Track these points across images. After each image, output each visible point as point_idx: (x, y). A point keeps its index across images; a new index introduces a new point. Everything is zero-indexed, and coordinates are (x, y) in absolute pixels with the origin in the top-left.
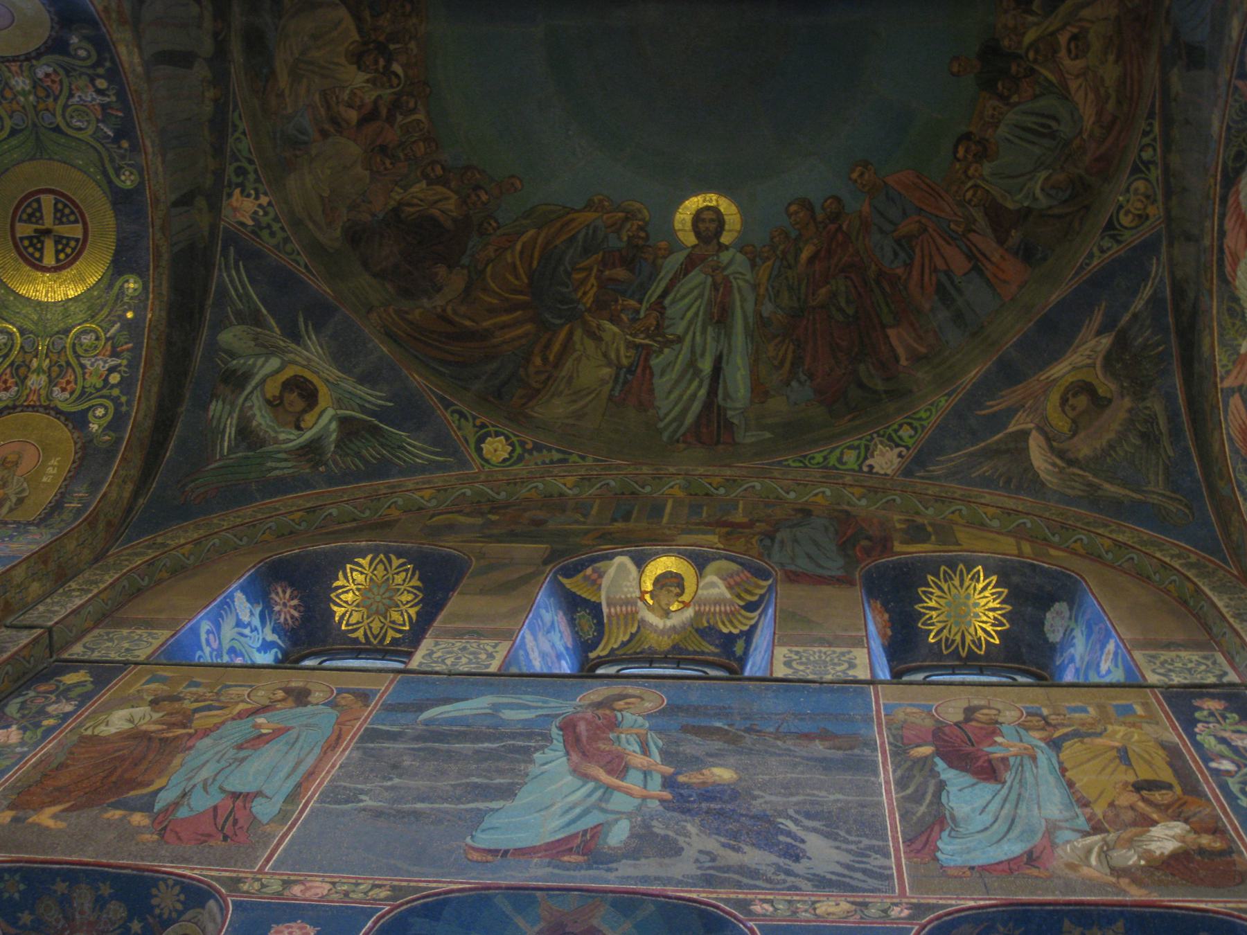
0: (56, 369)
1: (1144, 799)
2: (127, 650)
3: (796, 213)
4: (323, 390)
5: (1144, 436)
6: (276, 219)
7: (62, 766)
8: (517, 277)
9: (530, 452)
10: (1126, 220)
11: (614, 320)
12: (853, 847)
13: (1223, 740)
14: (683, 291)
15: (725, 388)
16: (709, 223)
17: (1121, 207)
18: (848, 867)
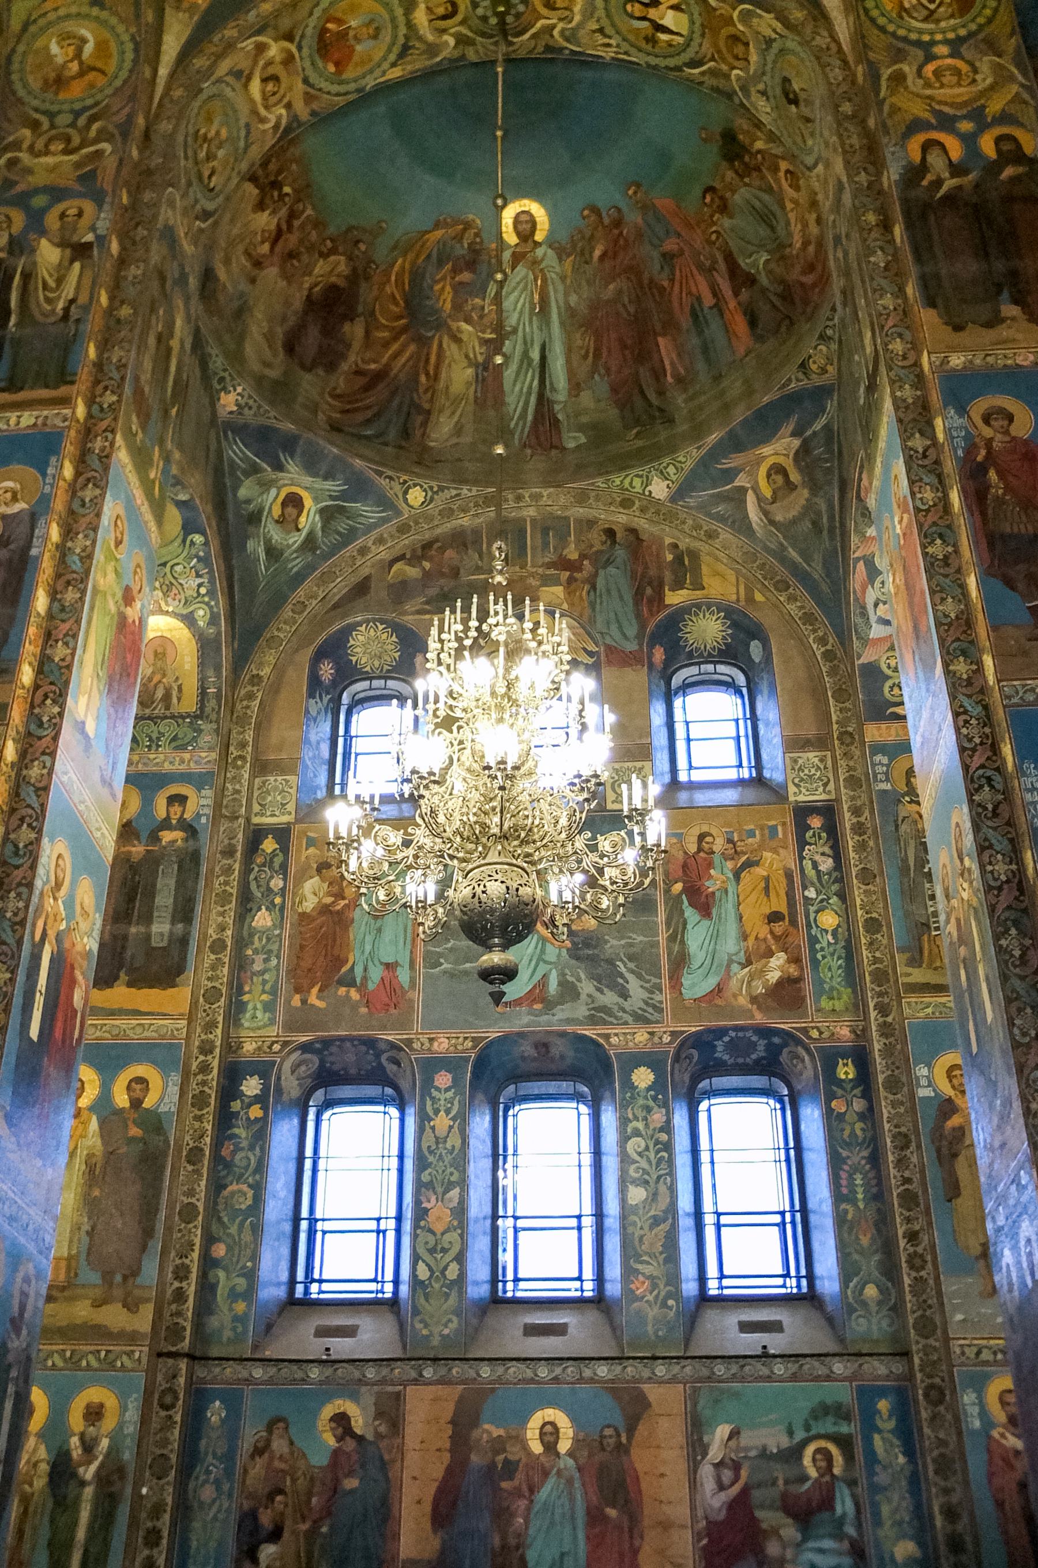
0: (165, 588)
1: (772, 932)
2: (283, 805)
3: (588, 216)
4: (304, 494)
5: (814, 523)
6: (250, 397)
7: (302, 947)
8: (397, 304)
9: (436, 493)
10: (814, 367)
11: (468, 320)
12: (647, 985)
13: (815, 866)
14: (513, 284)
15: (551, 384)
16: (525, 226)
17: (810, 357)
18: (647, 1003)
